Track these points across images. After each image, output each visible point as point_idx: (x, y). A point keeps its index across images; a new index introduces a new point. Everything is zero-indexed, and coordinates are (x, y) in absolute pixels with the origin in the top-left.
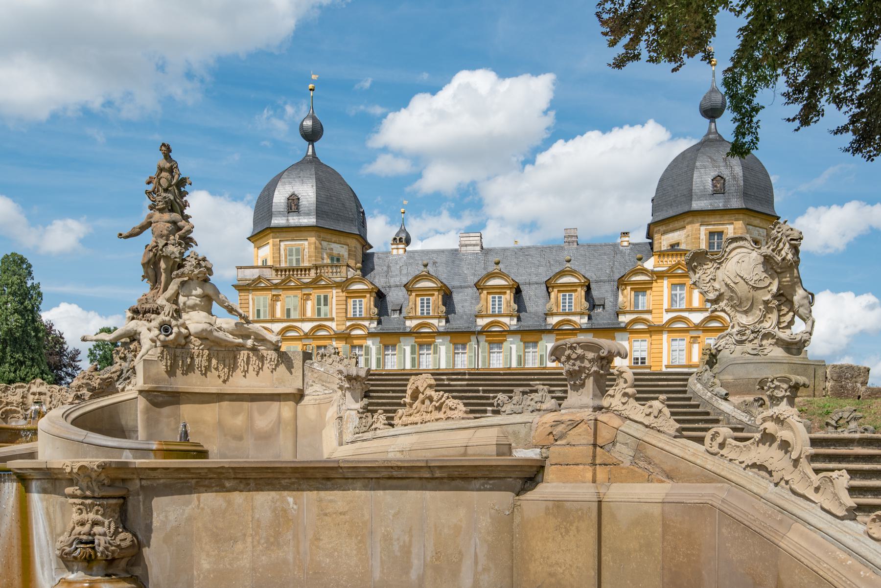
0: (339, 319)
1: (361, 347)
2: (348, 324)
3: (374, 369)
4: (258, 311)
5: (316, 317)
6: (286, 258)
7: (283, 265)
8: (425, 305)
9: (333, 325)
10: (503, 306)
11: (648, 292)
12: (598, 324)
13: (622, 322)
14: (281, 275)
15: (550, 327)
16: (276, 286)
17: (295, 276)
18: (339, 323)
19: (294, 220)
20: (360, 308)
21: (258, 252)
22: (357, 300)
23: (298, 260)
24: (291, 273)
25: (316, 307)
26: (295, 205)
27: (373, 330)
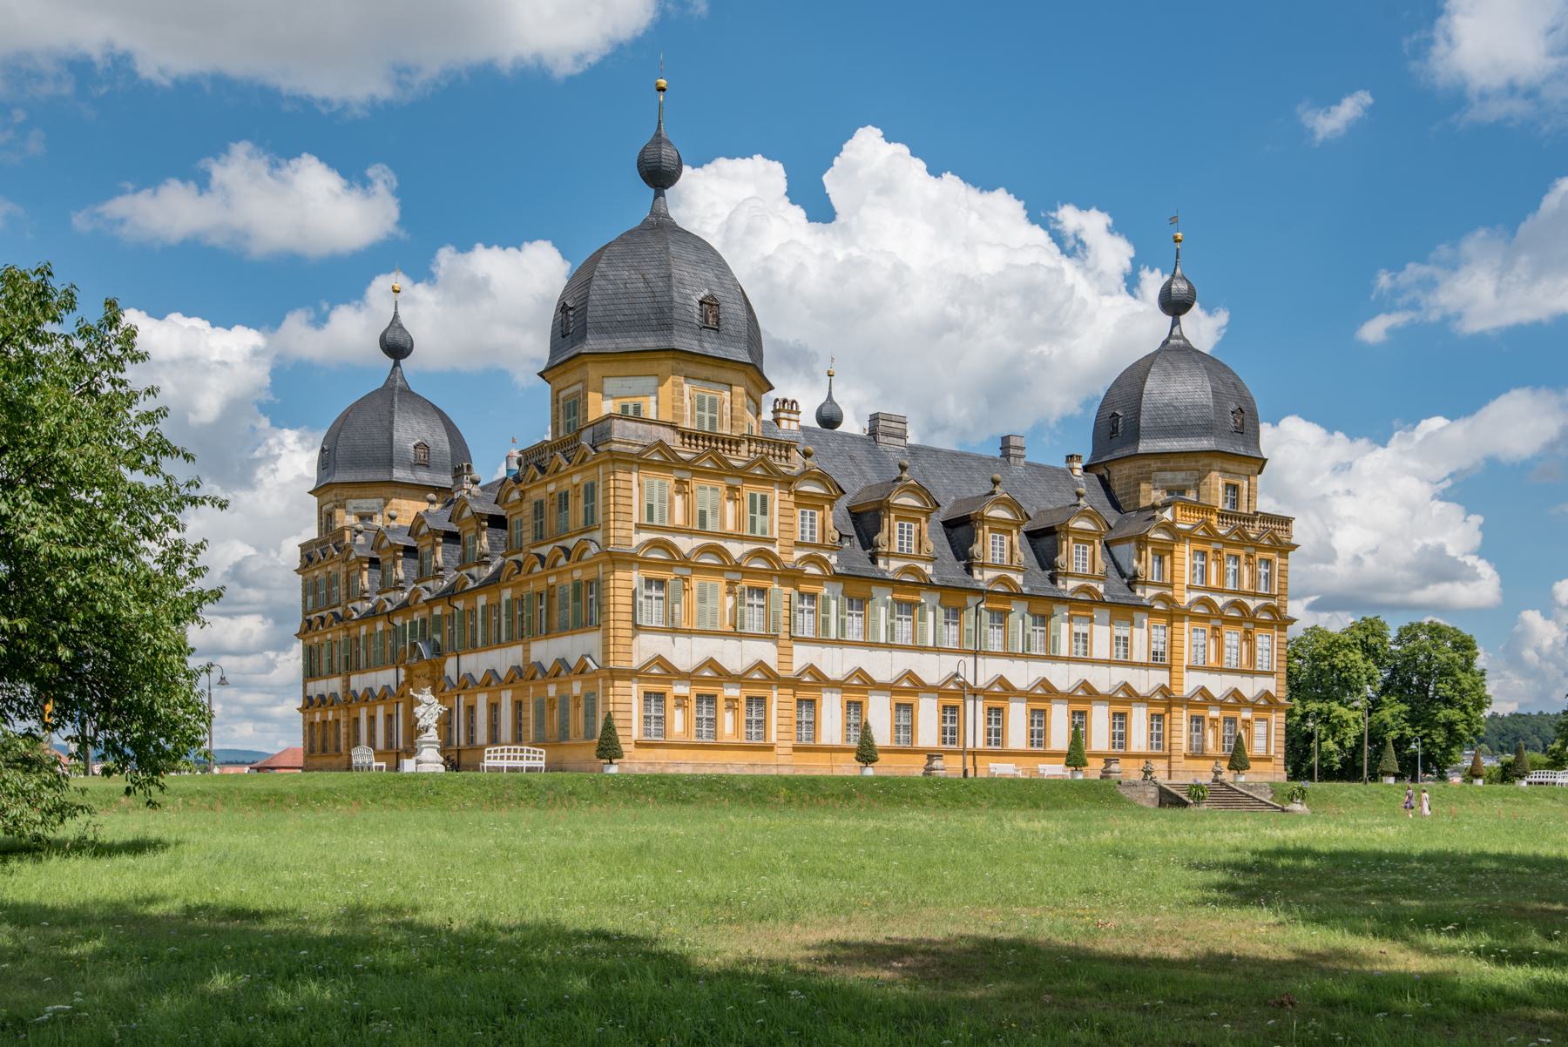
0: (784, 542)
1: (813, 597)
2: (798, 554)
3: (834, 637)
4: (650, 507)
5: (747, 533)
6: (692, 412)
7: (687, 424)
8: (906, 535)
9: (776, 550)
10: (1007, 553)
11: (1167, 558)
12: (1119, 598)
13: (1141, 598)
14: (690, 444)
15: (1068, 595)
16: (685, 465)
17: (720, 451)
18: (784, 549)
19: (711, 348)
20: (811, 526)
21: (603, 383)
22: (808, 511)
23: (712, 420)
24: (714, 445)
25: (748, 515)
26: (714, 316)
27: (838, 570)
